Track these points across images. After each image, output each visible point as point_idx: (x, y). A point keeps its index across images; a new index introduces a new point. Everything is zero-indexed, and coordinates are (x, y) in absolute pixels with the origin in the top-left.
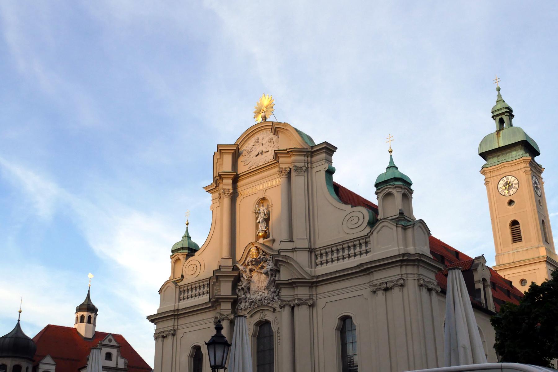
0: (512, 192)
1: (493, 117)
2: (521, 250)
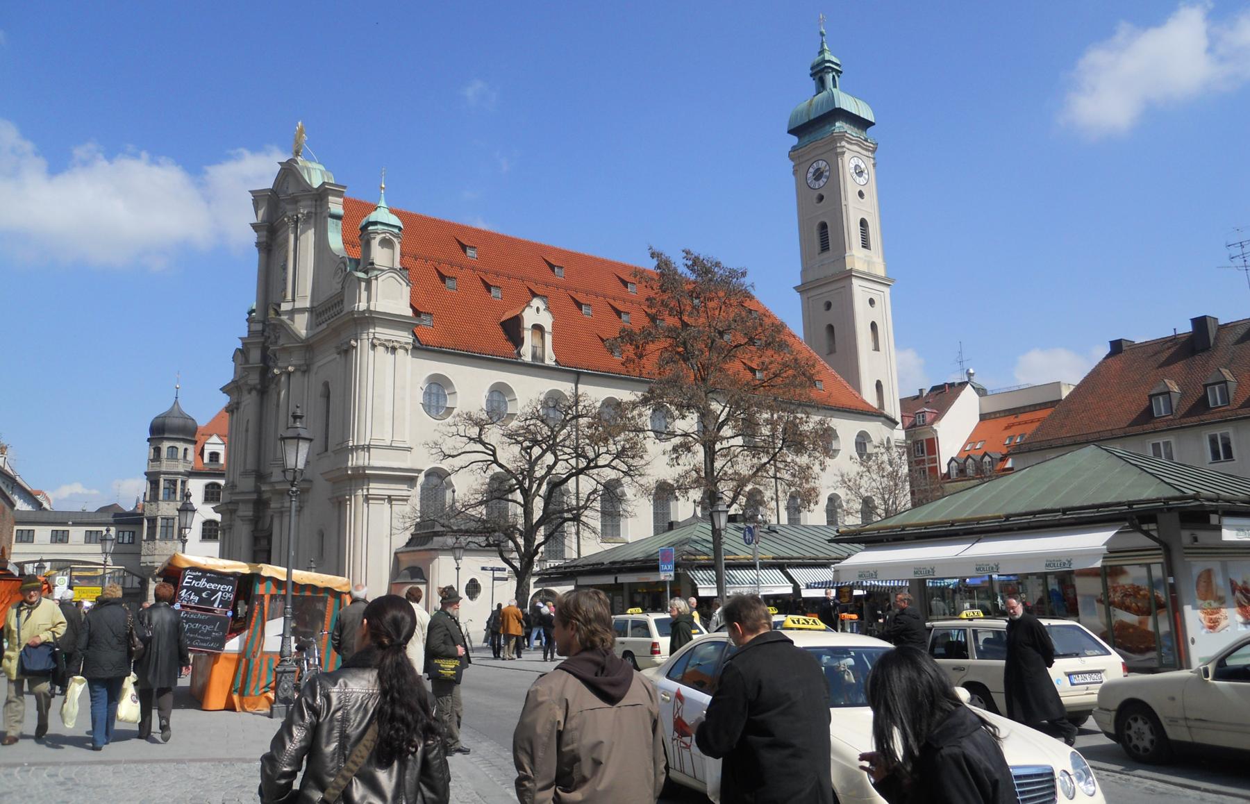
0: (821, 183)
1: (811, 75)
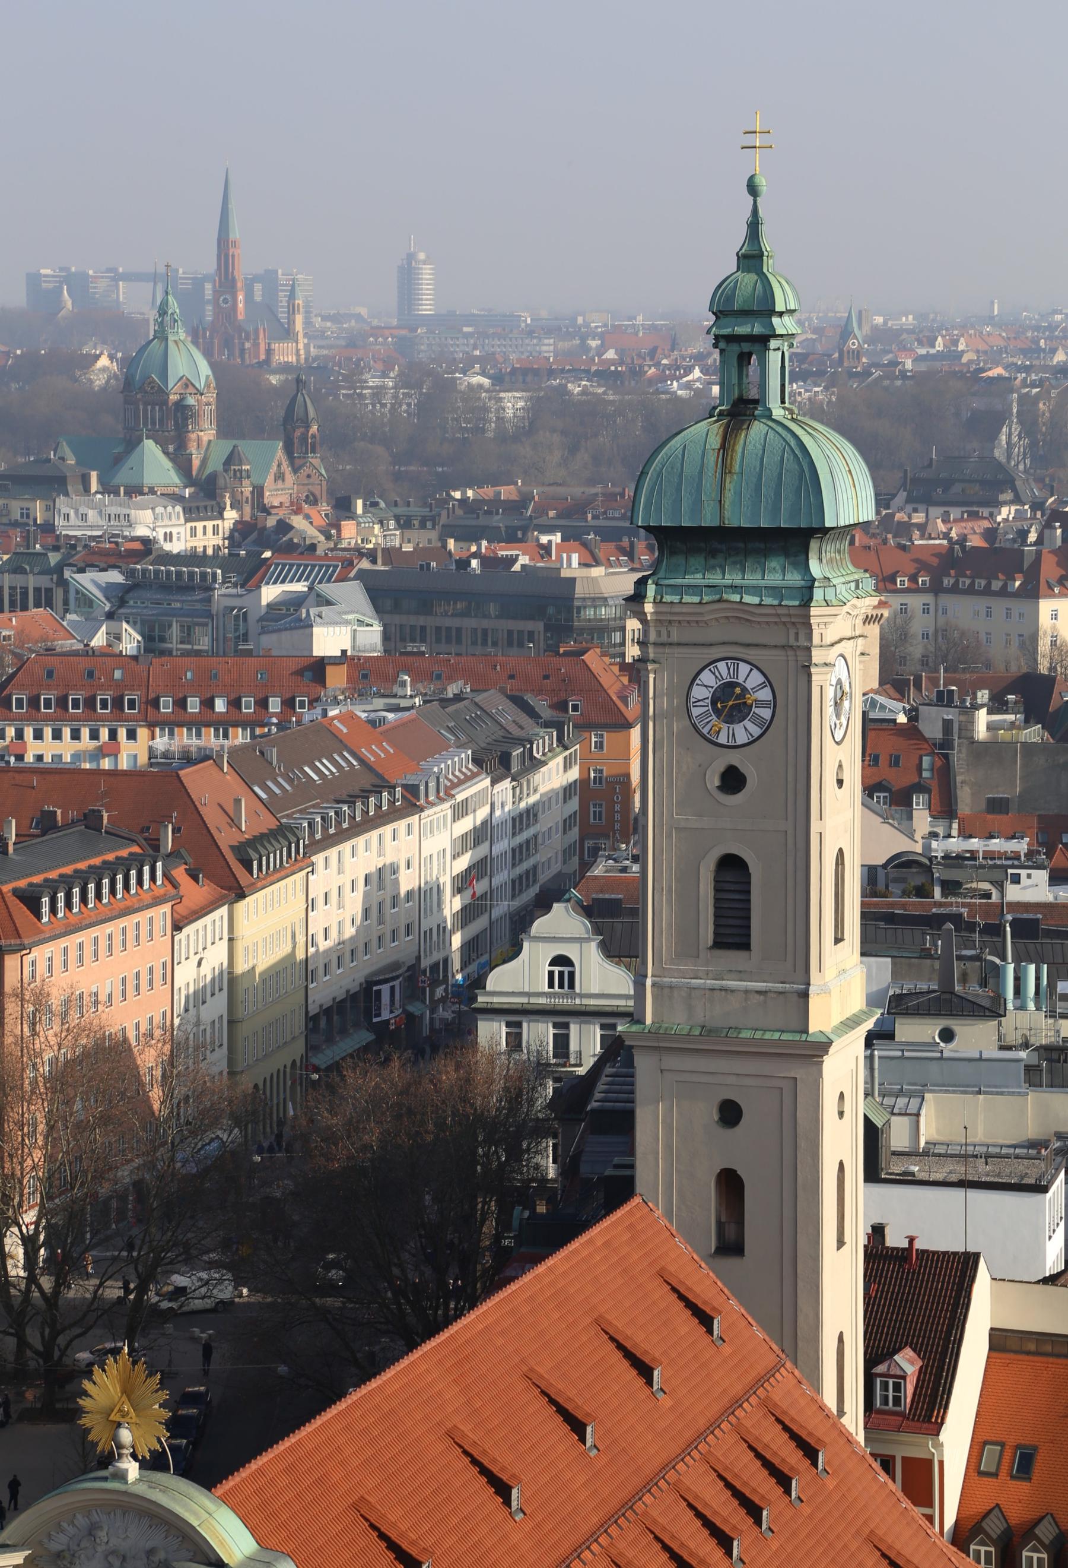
0: (742, 732)
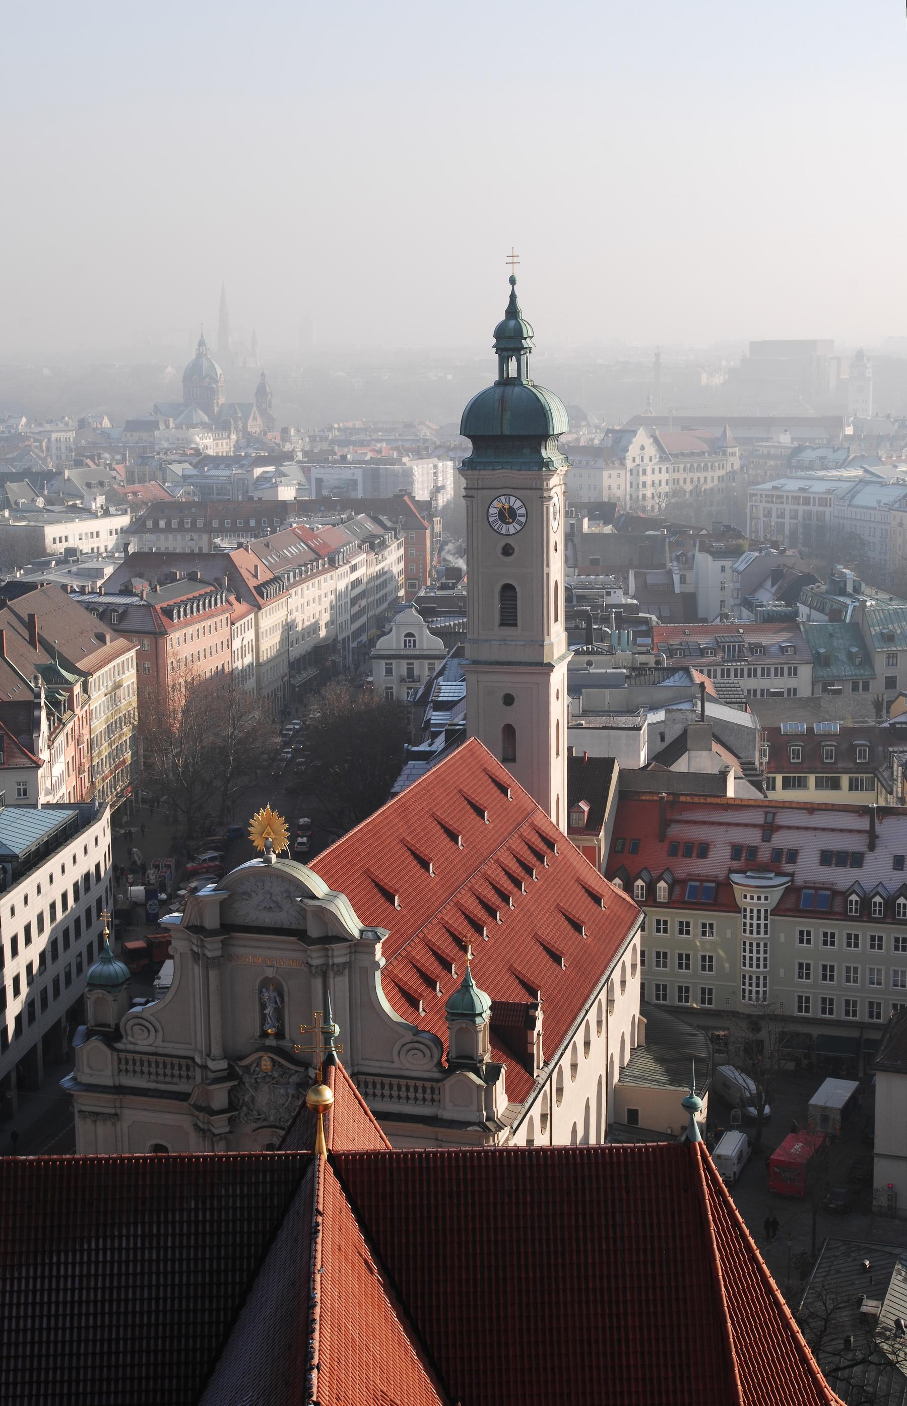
0: (512, 528)
2: (514, 643)
